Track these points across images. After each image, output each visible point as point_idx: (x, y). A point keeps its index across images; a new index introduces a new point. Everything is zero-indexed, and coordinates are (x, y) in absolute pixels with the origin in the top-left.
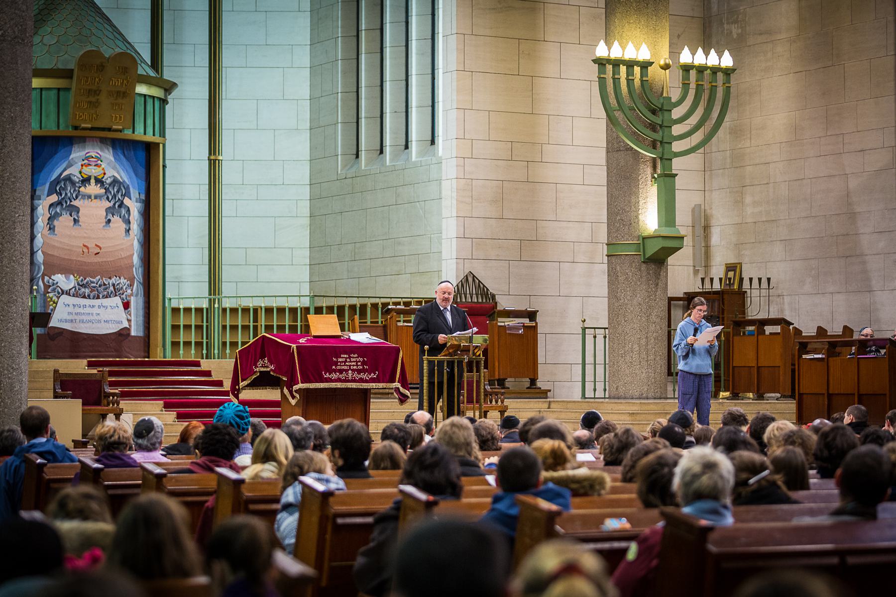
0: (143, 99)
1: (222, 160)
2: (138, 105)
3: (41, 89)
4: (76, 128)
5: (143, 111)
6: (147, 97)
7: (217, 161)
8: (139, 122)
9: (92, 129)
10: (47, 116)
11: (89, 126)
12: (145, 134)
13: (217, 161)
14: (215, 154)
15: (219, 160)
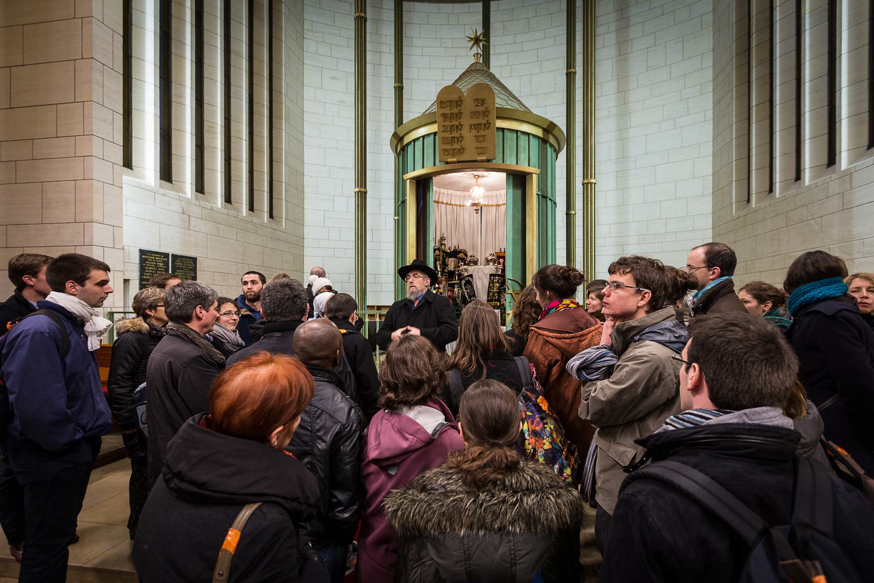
0: (515, 135)
1: (595, 184)
2: (509, 141)
3: (423, 137)
4: (447, 163)
5: (515, 146)
6: (519, 133)
7: (589, 184)
8: (510, 156)
9: (459, 162)
10: (427, 159)
11: (455, 160)
12: (517, 164)
13: (589, 184)
14: (587, 178)
15: (591, 183)
